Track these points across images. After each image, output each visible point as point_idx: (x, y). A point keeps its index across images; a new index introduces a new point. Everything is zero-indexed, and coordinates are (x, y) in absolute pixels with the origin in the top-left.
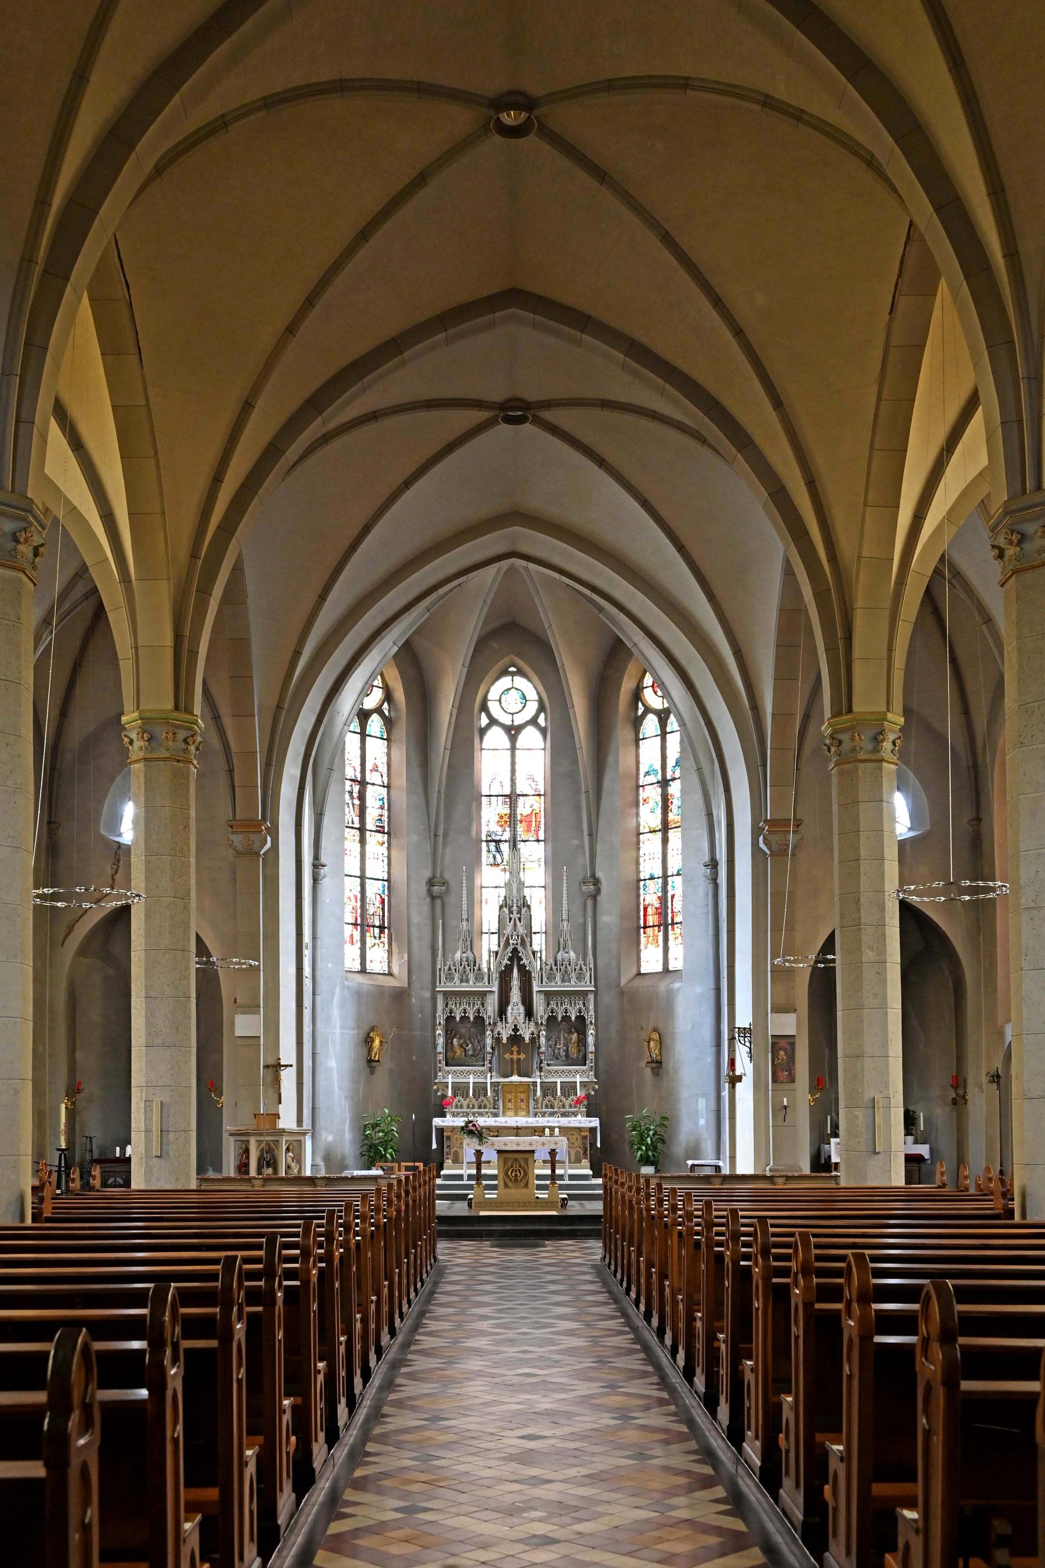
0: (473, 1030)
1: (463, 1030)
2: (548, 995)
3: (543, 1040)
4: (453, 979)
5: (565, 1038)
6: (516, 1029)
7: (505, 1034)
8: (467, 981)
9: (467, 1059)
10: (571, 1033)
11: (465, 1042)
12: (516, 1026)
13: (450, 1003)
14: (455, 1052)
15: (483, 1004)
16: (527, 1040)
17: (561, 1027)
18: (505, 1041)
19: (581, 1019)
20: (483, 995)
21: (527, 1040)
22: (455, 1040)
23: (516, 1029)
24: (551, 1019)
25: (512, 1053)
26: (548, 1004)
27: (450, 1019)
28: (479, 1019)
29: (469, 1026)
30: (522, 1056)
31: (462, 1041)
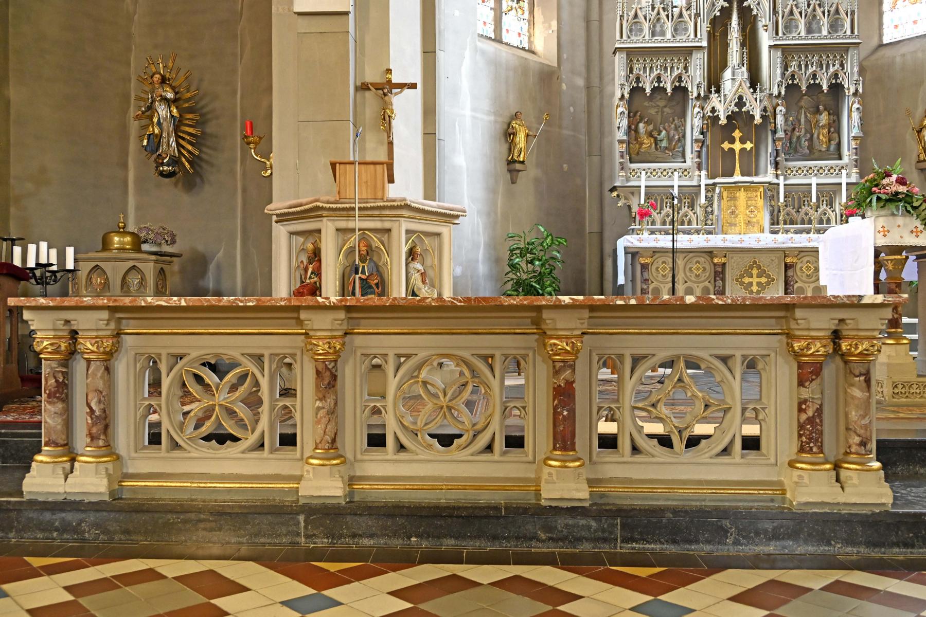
0: (667, 110)
1: (653, 111)
2: (787, 52)
3: (780, 119)
4: (641, 30)
5: (808, 121)
6: (740, 103)
7: (722, 107)
8: (663, 33)
9: (659, 154)
10: (818, 112)
11: (655, 129)
12: (740, 98)
13: (636, 66)
14: (641, 144)
15: (686, 68)
16: (758, 120)
17: (802, 103)
18: (723, 121)
19: (837, 88)
20: (687, 52)
21: (758, 120)
22: (641, 125)
23: (740, 103)
24: (792, 88)
25: (732, 141)
26: (786, 69)
27: (636, 91)
28: (681, 91)
29: (662, 103)
30: (749, 146)
31: (651, 127)
